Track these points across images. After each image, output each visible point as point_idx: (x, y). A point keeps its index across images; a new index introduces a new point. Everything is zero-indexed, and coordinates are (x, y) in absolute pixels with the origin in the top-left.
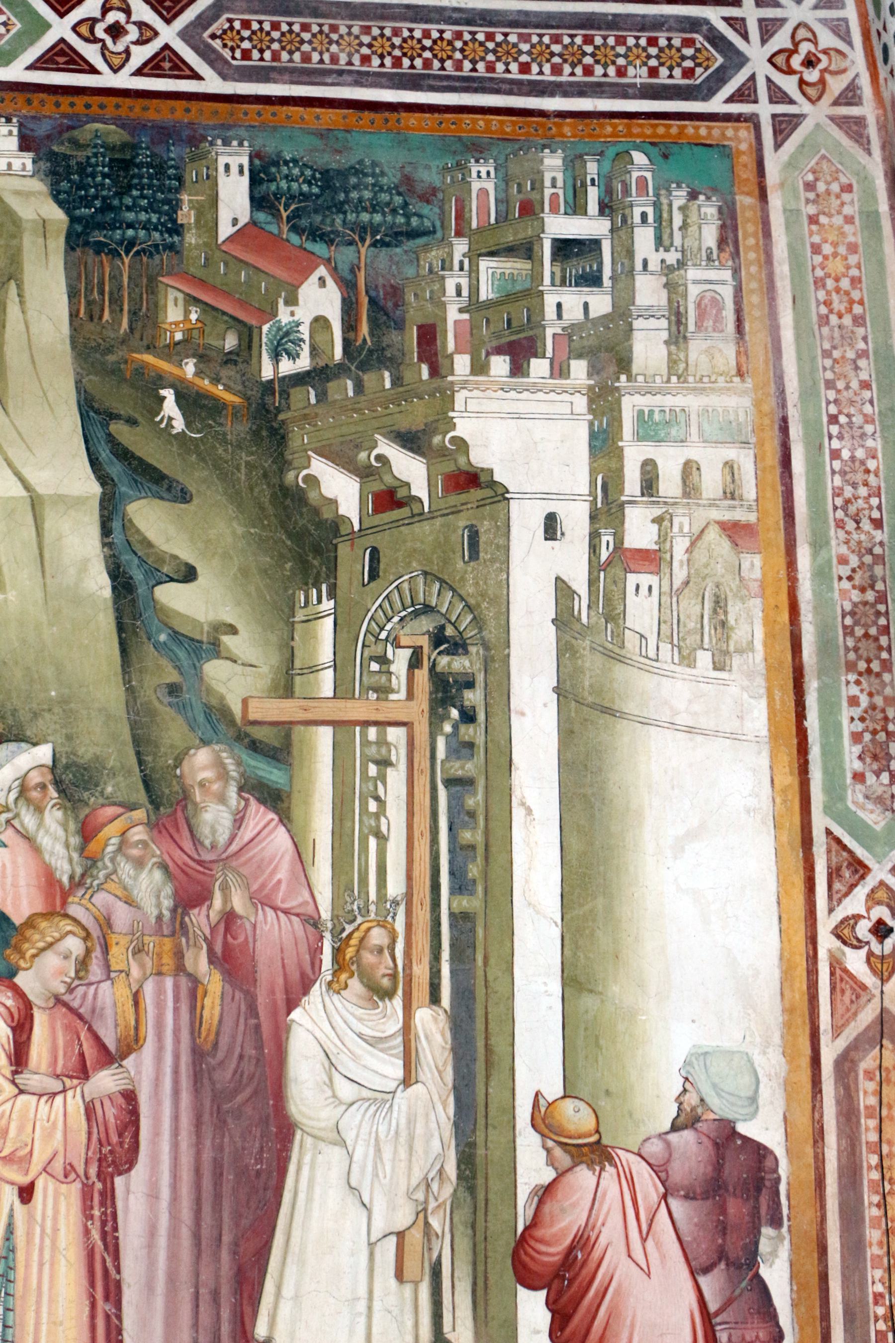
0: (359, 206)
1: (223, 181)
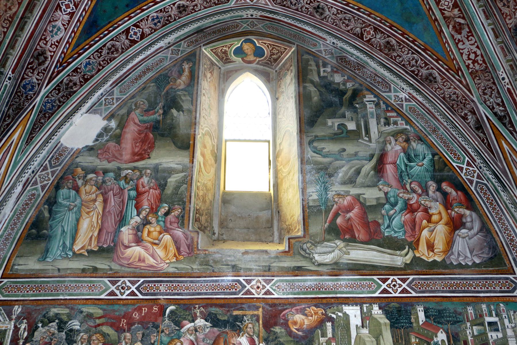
0: (447, 317)
1: (419, 313)
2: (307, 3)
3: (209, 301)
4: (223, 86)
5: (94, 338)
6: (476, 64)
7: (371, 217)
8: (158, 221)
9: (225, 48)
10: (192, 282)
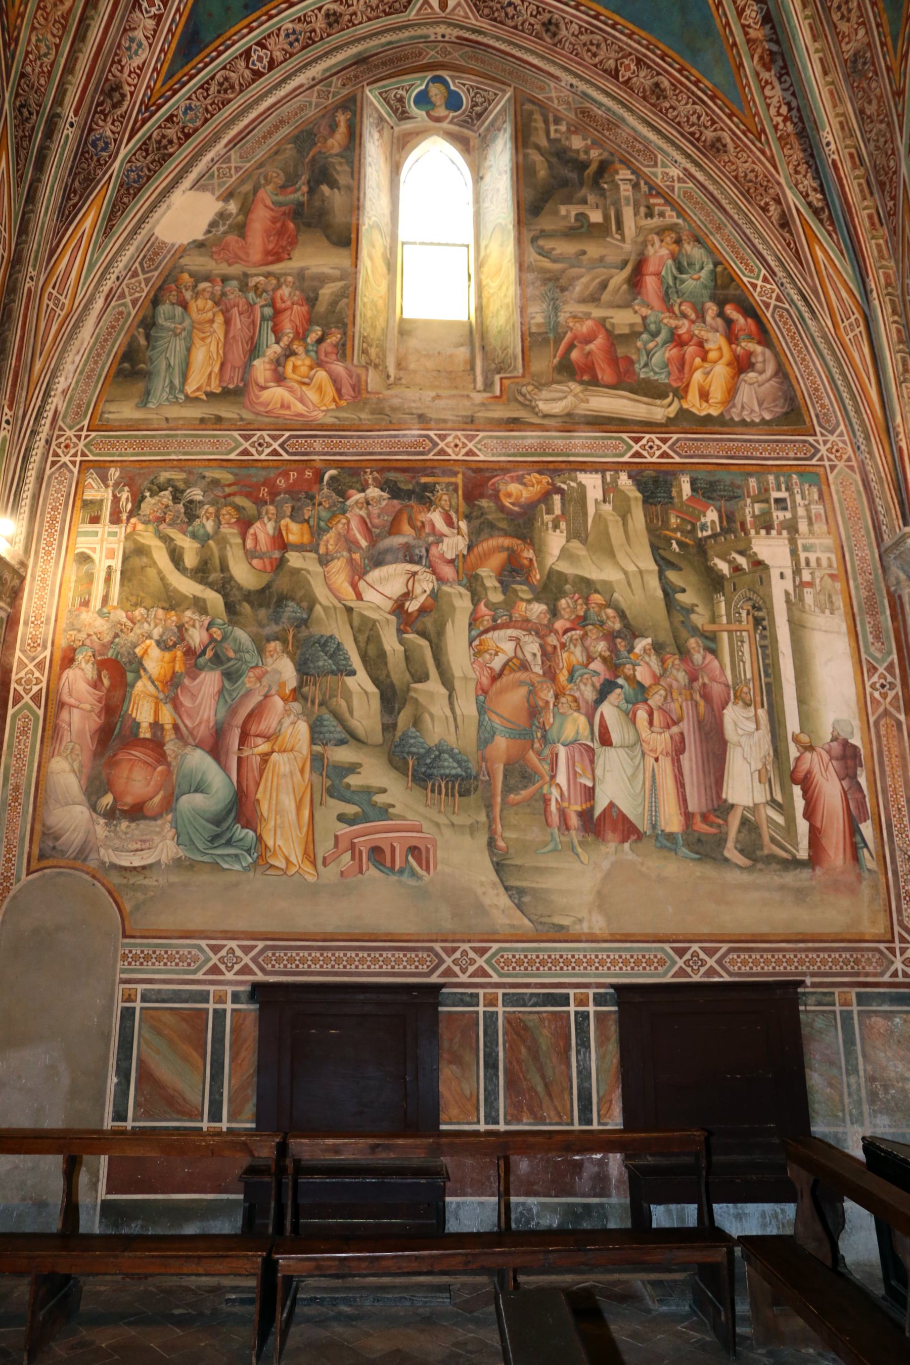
2: (531, 15)
3: (386, 464)
4: (397, 157)
5: (224, 511)
6: (788, 124)
7: (621, 351)
8: (307, 352)
9: (400, 92)
10: (359, 437)
